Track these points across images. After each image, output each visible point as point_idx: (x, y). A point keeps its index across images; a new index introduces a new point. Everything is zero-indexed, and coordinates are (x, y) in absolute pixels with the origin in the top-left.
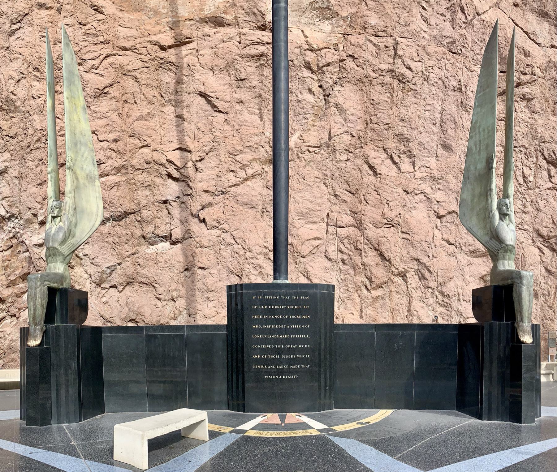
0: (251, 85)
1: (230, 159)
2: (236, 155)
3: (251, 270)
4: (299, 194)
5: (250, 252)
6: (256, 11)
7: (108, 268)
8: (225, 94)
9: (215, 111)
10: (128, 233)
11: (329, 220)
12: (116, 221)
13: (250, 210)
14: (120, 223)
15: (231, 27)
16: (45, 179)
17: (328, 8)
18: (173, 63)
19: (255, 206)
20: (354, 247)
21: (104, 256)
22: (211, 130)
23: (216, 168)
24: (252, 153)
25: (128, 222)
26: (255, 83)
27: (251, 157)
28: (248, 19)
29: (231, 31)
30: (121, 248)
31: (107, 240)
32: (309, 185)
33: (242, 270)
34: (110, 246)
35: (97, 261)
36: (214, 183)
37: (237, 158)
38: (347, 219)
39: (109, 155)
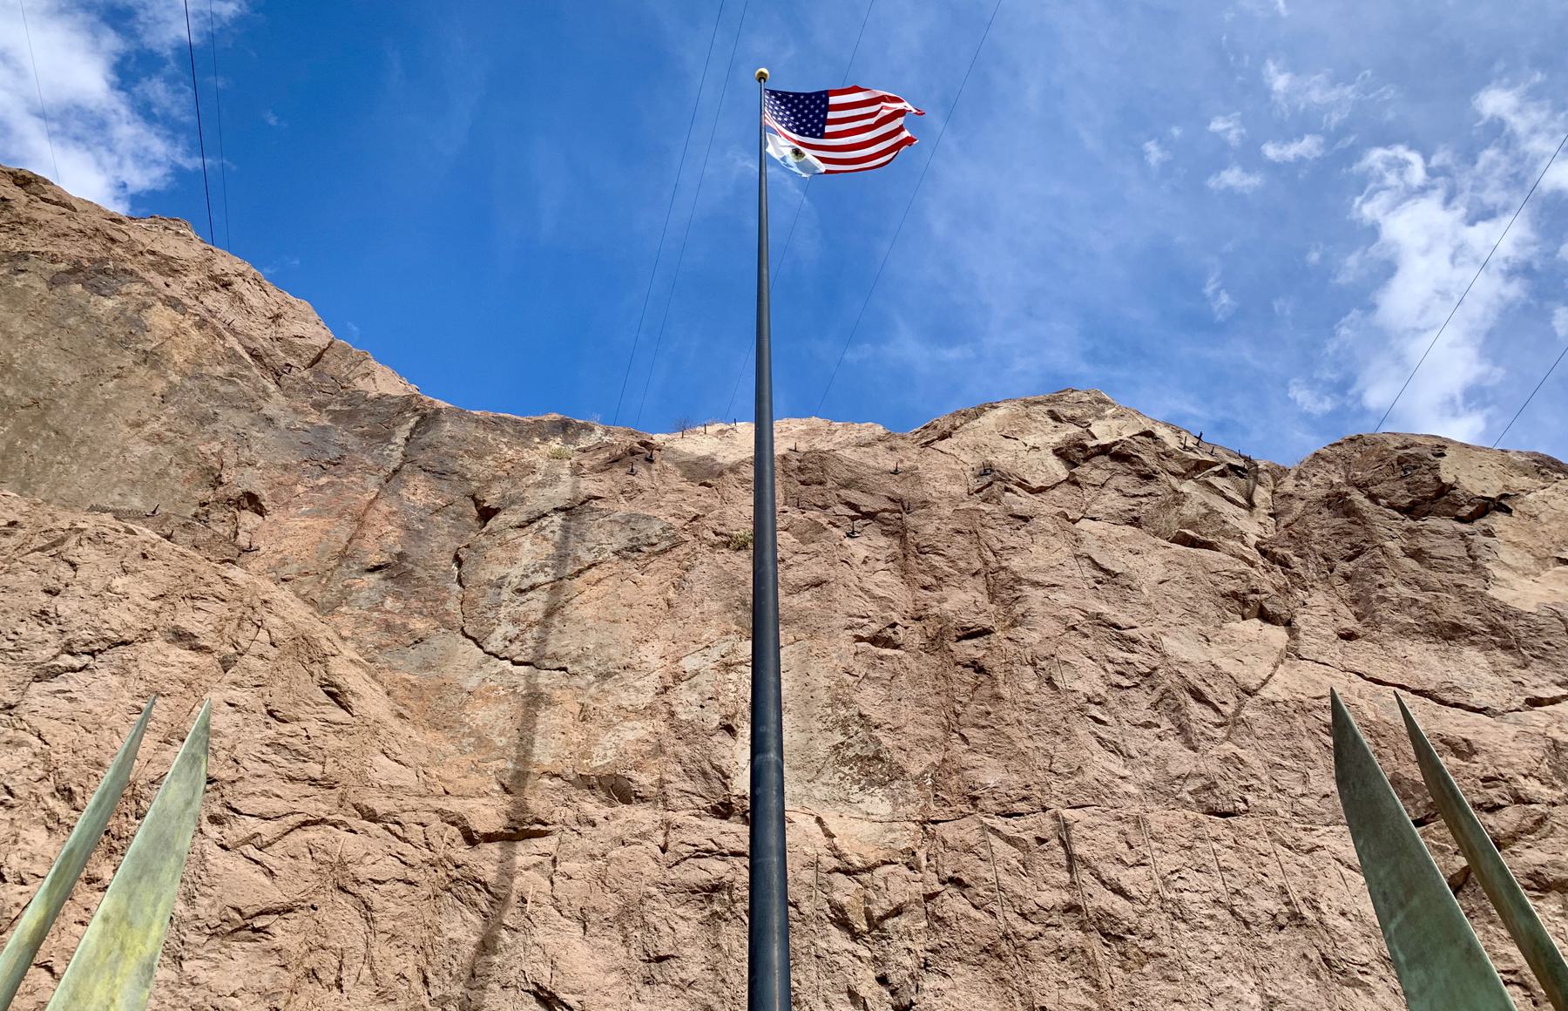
0: (683, 975)
6: (708, 768)
8: (607, 1000)
26: (694, 971)
28: (688, 786)
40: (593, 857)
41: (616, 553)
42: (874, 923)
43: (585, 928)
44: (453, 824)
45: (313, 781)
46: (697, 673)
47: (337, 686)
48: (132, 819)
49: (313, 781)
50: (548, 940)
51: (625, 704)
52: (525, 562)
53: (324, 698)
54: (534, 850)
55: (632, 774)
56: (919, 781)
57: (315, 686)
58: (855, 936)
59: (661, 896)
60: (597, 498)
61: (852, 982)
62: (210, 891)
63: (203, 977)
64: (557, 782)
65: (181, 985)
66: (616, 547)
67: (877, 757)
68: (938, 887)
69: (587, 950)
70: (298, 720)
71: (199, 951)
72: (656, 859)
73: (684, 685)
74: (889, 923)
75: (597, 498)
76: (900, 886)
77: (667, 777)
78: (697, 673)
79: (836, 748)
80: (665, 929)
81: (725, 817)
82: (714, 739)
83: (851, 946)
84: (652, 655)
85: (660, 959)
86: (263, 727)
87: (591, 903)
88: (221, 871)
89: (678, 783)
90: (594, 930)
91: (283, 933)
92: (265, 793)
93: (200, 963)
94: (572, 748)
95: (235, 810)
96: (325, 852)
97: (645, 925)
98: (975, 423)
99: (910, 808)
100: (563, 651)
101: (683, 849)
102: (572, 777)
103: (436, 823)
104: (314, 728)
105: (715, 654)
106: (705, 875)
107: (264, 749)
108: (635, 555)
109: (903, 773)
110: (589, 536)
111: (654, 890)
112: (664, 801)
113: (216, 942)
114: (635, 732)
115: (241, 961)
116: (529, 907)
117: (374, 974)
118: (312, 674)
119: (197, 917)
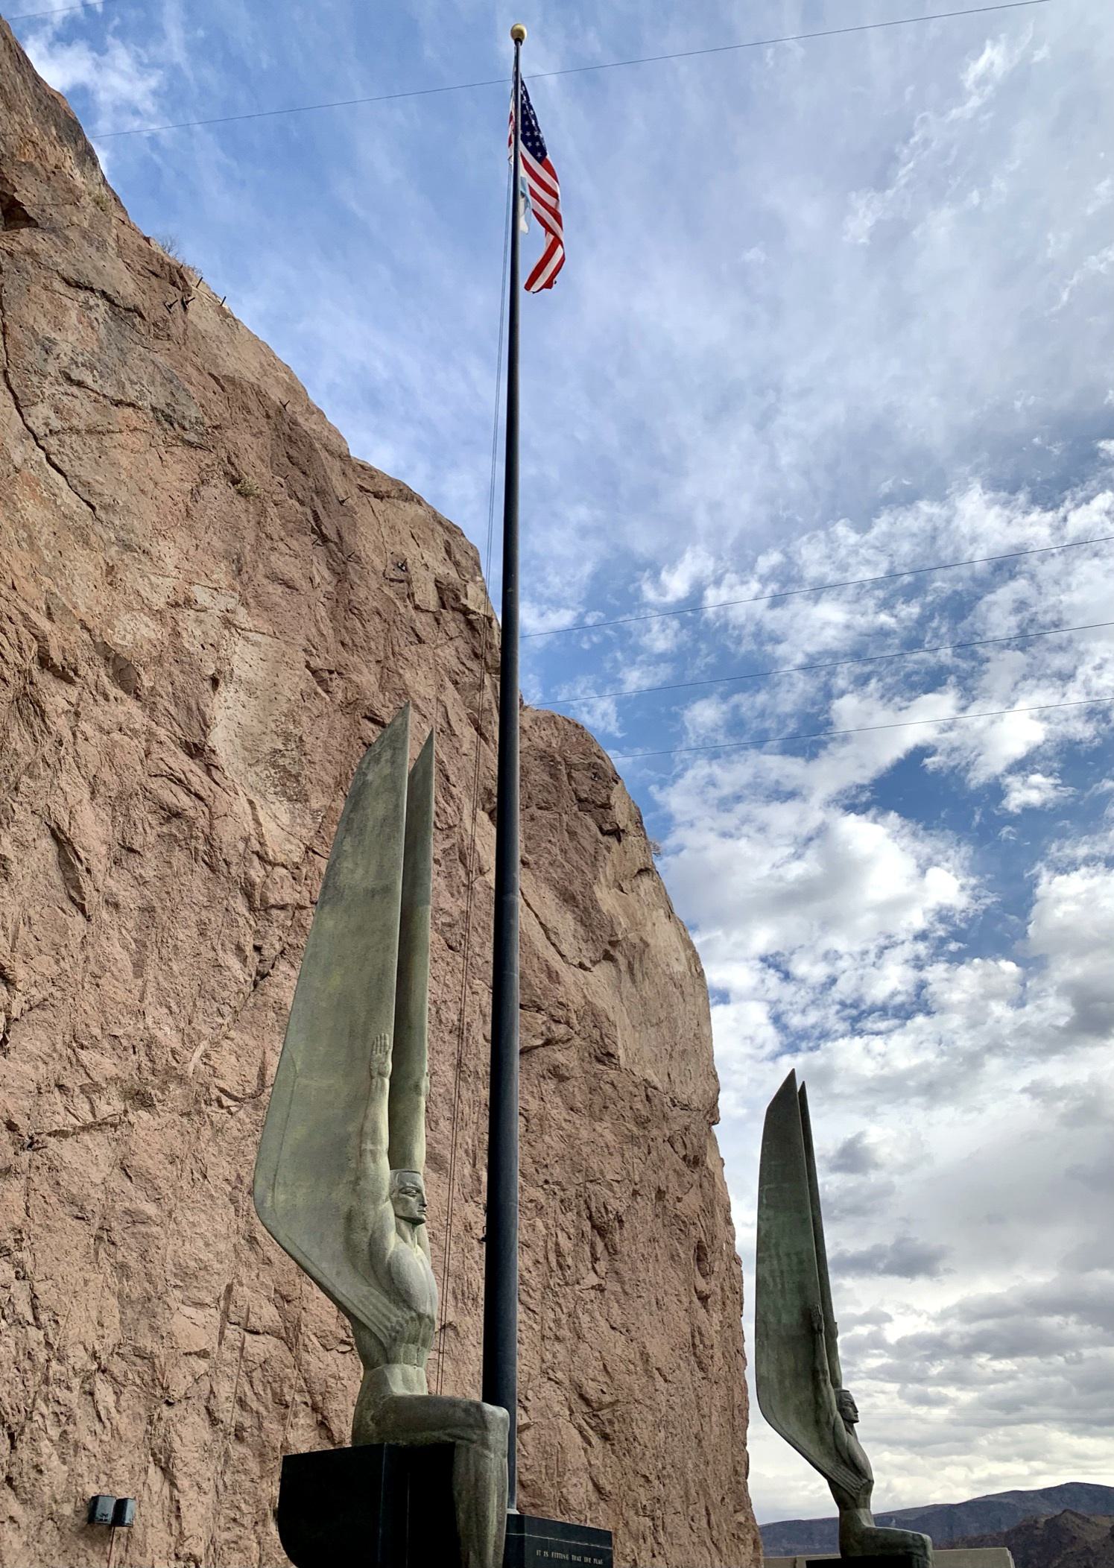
2: (82, 1047)
3: (48, 1423)
4: (188, 1213)
5: (60, 1361)
9: (71, 898)
11: (232, 1308)
13: (75, 1223)
15: (139, 704)
17: (296, 778)
18: (43, 711)
20: (274, 1394)
22: (55, 947)
23: (40, 1064)
24: (116, 1060)
28: (172, 709)
32: (212, 1196)
36: (27, 1104)
37: (83, 1055)
38: (268, 1314)
42: (267, 908)
43: (93, 793)
51: (143, 593)
56: (314, 813)
58: (252, 909)
61: (242, 940)
64: (86, 636)
67: (296, 778)
68: (308, 904)
74: (274, 912)
76: (284, 892)
79: (276, 751)
81: (191, 756)
83: (247, 914)
84: (169, 552)
85: (131, 850)
98: (402, 504)
99: (304, 832)
102: (98, 640)
106: (175, 801)
109: (307, 801)
112: (152, 710)
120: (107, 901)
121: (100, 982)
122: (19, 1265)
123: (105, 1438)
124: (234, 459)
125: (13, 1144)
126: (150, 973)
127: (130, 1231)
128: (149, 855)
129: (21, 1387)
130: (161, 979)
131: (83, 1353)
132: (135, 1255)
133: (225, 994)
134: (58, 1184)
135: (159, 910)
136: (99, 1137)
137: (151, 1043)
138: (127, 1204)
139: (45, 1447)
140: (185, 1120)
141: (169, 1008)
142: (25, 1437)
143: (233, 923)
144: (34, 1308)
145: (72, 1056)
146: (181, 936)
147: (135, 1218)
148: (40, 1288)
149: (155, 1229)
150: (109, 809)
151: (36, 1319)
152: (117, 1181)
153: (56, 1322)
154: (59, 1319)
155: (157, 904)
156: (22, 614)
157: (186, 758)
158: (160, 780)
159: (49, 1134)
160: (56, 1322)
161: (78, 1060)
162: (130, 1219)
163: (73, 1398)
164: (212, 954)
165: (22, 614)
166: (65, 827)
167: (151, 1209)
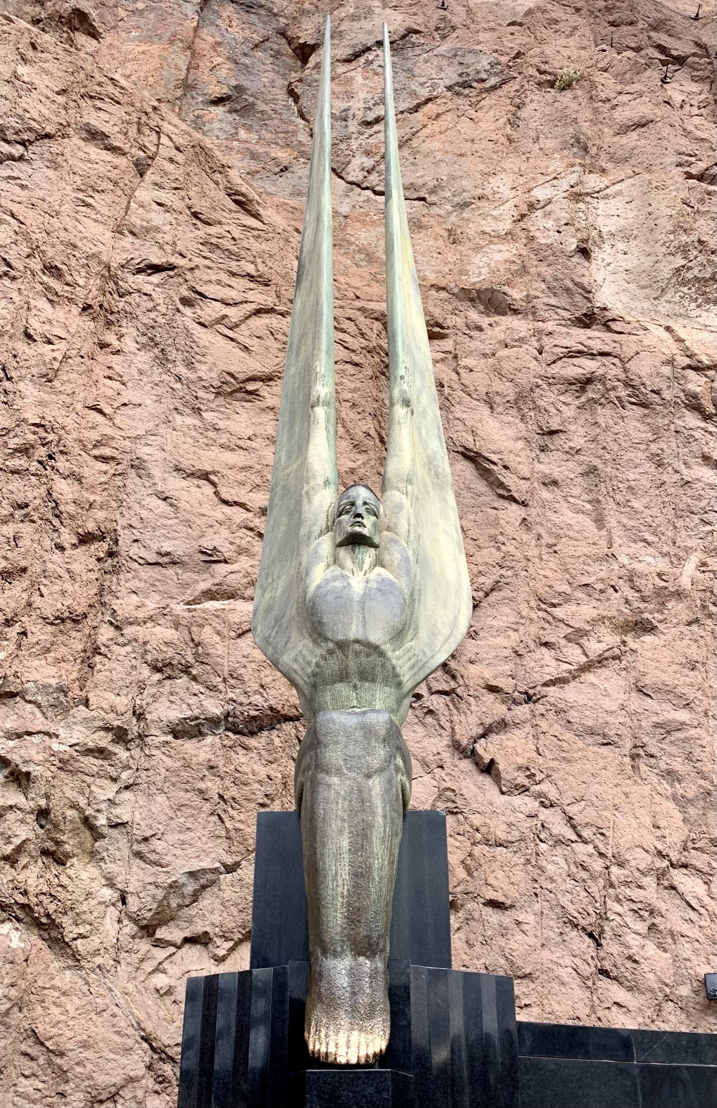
1: (540, 614)
2: (554, 606)
3: (628, 920)
5: (621, 865)
6: (571, 285)
7: (192, 874)
8: (520, 459)
9: (501, 496)
10: (273, 774)
12: (236, 732)
13: (604, 750)
14: (252, 742)
16: (23, 563)
19: (616, 739)
21: (182, 837)
22: (493, 538)
23: (511, 633)
25: (277, 742)
27: (594, 613)
28: (553, 301)
29: (520, 326)
30: (242, 817)
31: (202, 785)
33: (603, 917)
34: (207, 807)
35: (159, 849)
36: (507, 668)
39: (243, 543)
40: (485, 355)
41: (449, 88)
43: (491, 407)
44: (377, 319)
45: (251, 277)
46: (550, 202)
47: (243, 195)
48: (116, 296)
49: (251, 277)
50: (464, 416)
51: (488, 230)
52: (362, 95)
53: (234, 206)
54: (438, 348)
55: (506, 289)
57: (222, 194)
59: (545, 386)
60: (417, 32)
62: (203, 359)
63: (221, 424)
65: (207, 430)
66: (448, 82)
69: (497, 425)
70: (220, 223)
71: (211, 405)
72: (536, 359)
73: (539, 213)
75: (417, 32)
77: (533, 293)
78: (550, 202)
80: (553, 410)
82: (573, 259)
84: (502, 184)
85: (552, 433)
86: (192, 228)
87: (495, 389)
88: (207, 344)
89: (544, 299)
90: (500, 409)
91: (270, 395)
92: (219, 282)
93: (215, 414)
94: (451, 266)
95: (200, 294)
96: (284, 334)
97: (536, 408)
100: (420, 182)
101: (558, 350)
103: (361, 320)
104: (237, 233)
105: (564, 184)
107: (201, 247)
108: (467, 91)
110: (417, 71)
111: (540, 382)
112: (534, 313)
113: (221, 400)
114: (500, 255)
115: (245, 415)
116: (447, 390)
117: (347, 431)
118: (217, 183)
119: (201, 379)
120: (544, 484)
121: (556, 548)
122: (539, 795)
123: (702, 923)
124: (544, 67)
125: (504, 702)
126: (612, 521)
127: (667, 740)
128: (573, 428)
129: (585, 894)
130: (625, 521)
131: (645, 855)
132: (679, 760)
133: (703, 504)
134: (569, 722)
135: (601, 466)
136: (604, 672)
137: (631, 578)
138: (655, 719)
139: (633, 940)
140: (694, 628)
141: (645, 541)
142: (608, 934)
143: (689, 440)
144: (574, 827)
145: (545, 615)
146: (632, 476)
147: (667, 729)
148: (573, 810)
149: (693, 732)
150: (514, 412)
151: (579, 836)
152: (636, 702)
153: (602, 834)
154: (604, 831)
155: (597, 462)
156: (359, 309)
157: (582, 331)
158: (559, 363)
159: (545, 685)
160: (602, 834)
161: (554, 618)
162: (663, 731)
163: (651, 893)
164: (676, 477)
165: (359, 309)
166: (471, 445)
167: (683, 716)
